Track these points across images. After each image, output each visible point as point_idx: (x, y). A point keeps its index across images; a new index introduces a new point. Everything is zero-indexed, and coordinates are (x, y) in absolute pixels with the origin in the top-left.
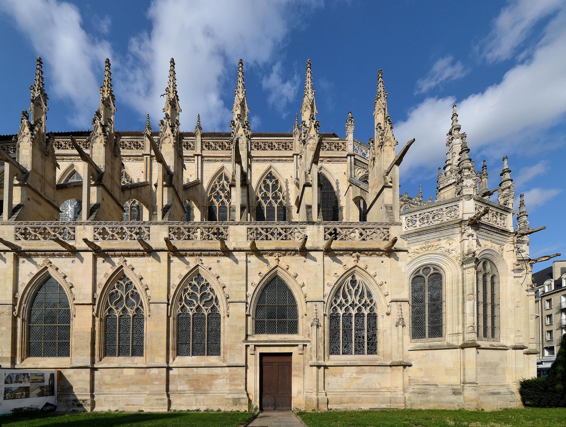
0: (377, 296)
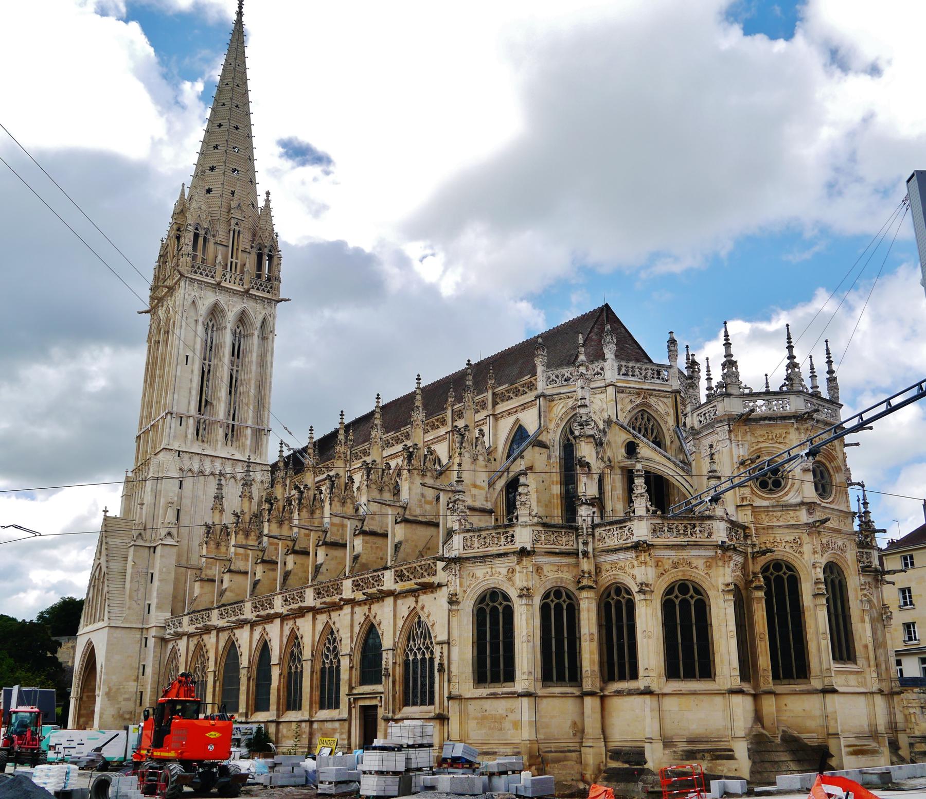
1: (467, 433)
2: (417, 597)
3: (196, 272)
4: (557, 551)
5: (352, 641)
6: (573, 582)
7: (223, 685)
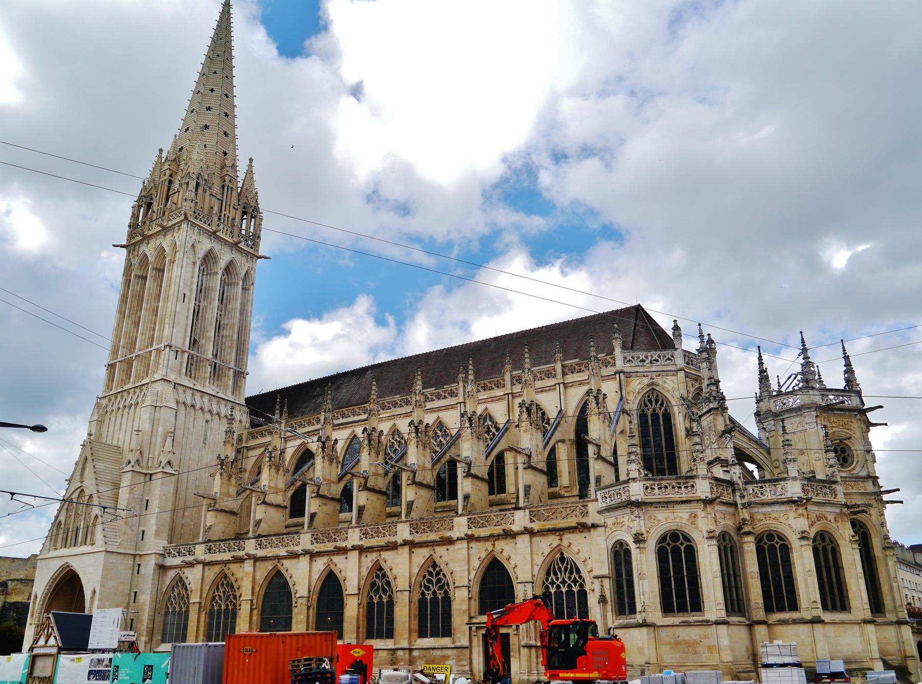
0: (584, 574)
1: (599, 395)
3: (196, 218)
4: (724, 501)
5: (469, 574)
6: (734, 528)
7: (263, 612)
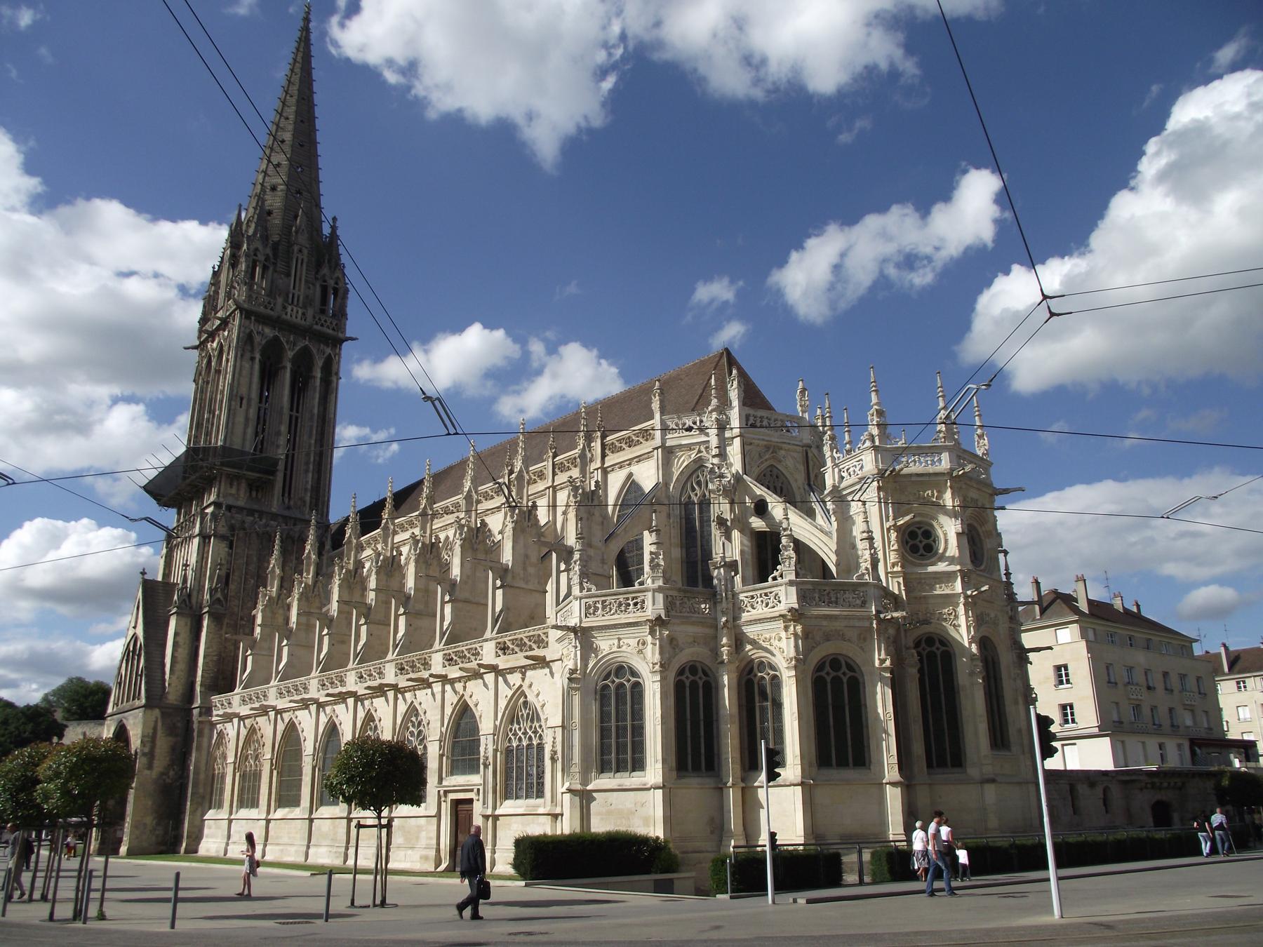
2: (524, 674)
5: (442, 725)
